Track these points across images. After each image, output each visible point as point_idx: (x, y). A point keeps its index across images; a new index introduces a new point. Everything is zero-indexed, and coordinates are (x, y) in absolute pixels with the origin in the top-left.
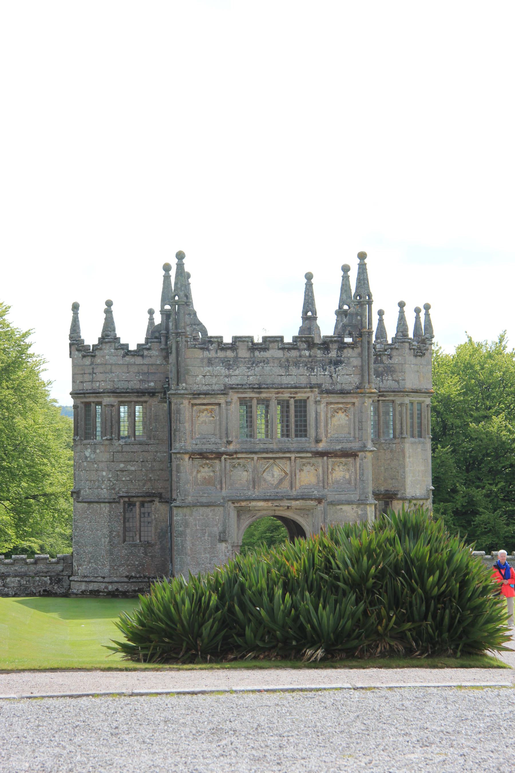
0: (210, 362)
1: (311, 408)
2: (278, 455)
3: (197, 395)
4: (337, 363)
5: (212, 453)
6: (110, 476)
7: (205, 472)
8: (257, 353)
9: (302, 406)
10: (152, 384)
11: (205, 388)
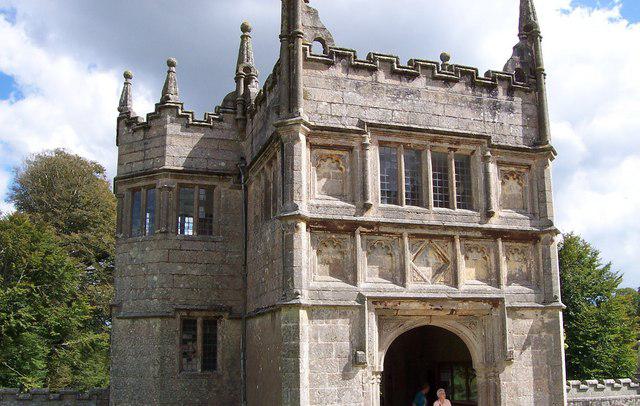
1: (477, 164)
2: (436, 233)
3: (316, 131)
5: (342, 222)
6: (164, 281)
7: (329, 253)
9: (464, 166)
10: (223, 164)
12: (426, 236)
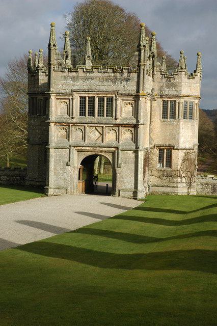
0: (65, 78)
2: (97, 125)
3: (58, 94)
4: (127, 80)
8: (88, 74)
9: (110, 100)
11: (62, 91)
12: (95, 125)
